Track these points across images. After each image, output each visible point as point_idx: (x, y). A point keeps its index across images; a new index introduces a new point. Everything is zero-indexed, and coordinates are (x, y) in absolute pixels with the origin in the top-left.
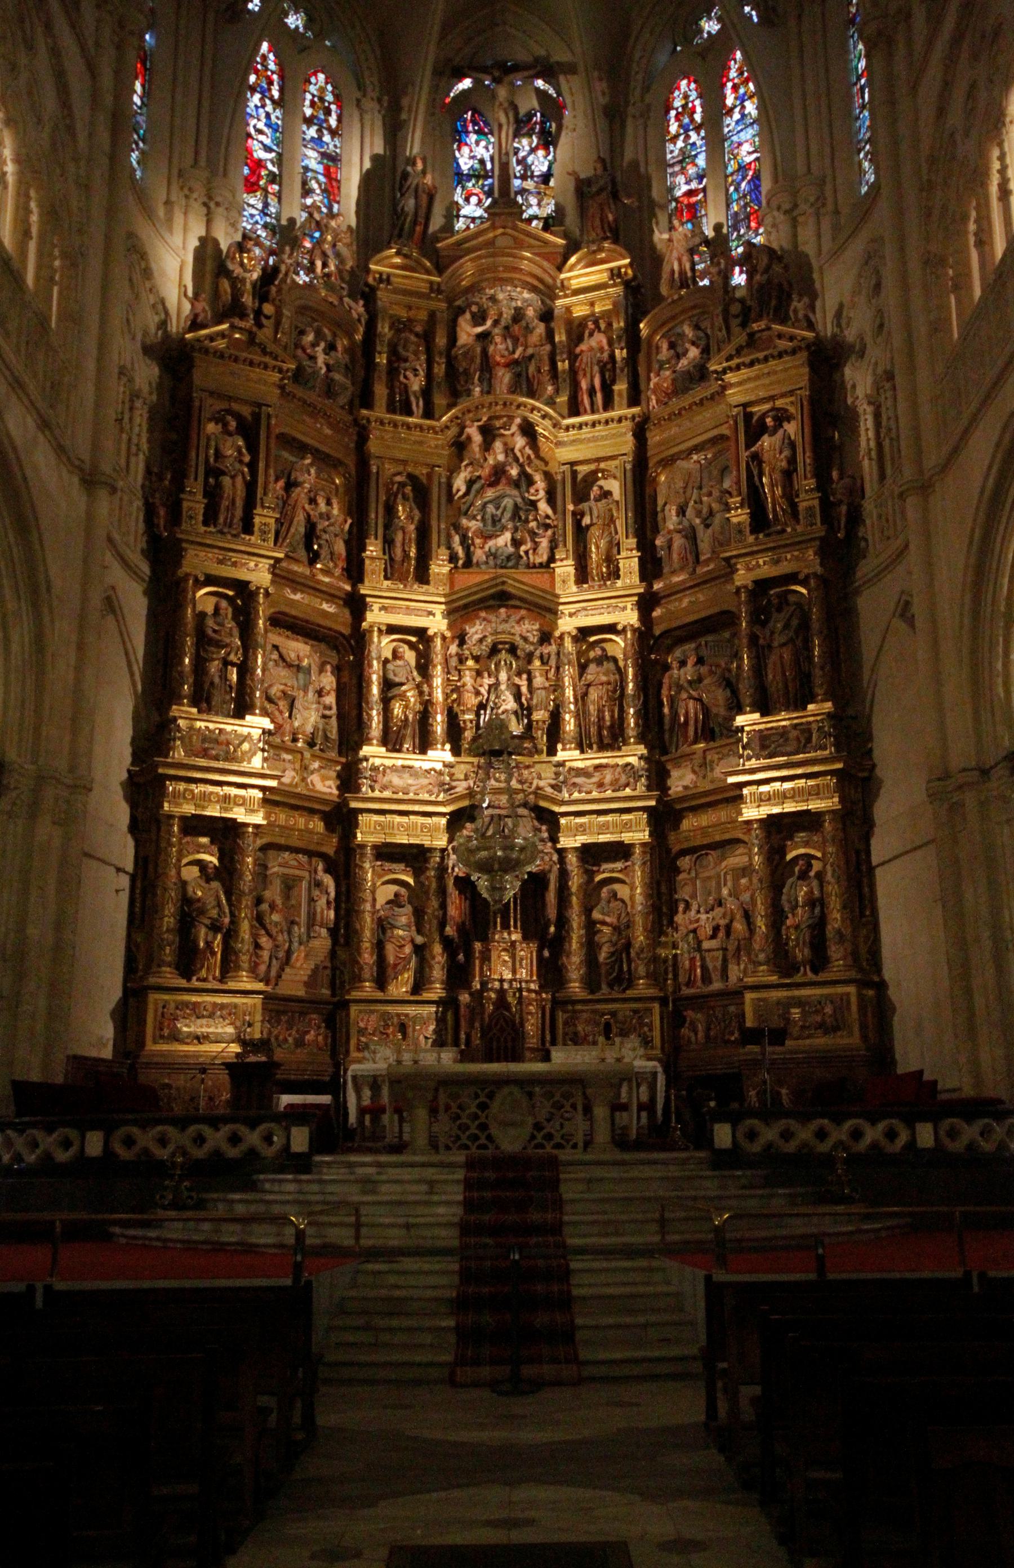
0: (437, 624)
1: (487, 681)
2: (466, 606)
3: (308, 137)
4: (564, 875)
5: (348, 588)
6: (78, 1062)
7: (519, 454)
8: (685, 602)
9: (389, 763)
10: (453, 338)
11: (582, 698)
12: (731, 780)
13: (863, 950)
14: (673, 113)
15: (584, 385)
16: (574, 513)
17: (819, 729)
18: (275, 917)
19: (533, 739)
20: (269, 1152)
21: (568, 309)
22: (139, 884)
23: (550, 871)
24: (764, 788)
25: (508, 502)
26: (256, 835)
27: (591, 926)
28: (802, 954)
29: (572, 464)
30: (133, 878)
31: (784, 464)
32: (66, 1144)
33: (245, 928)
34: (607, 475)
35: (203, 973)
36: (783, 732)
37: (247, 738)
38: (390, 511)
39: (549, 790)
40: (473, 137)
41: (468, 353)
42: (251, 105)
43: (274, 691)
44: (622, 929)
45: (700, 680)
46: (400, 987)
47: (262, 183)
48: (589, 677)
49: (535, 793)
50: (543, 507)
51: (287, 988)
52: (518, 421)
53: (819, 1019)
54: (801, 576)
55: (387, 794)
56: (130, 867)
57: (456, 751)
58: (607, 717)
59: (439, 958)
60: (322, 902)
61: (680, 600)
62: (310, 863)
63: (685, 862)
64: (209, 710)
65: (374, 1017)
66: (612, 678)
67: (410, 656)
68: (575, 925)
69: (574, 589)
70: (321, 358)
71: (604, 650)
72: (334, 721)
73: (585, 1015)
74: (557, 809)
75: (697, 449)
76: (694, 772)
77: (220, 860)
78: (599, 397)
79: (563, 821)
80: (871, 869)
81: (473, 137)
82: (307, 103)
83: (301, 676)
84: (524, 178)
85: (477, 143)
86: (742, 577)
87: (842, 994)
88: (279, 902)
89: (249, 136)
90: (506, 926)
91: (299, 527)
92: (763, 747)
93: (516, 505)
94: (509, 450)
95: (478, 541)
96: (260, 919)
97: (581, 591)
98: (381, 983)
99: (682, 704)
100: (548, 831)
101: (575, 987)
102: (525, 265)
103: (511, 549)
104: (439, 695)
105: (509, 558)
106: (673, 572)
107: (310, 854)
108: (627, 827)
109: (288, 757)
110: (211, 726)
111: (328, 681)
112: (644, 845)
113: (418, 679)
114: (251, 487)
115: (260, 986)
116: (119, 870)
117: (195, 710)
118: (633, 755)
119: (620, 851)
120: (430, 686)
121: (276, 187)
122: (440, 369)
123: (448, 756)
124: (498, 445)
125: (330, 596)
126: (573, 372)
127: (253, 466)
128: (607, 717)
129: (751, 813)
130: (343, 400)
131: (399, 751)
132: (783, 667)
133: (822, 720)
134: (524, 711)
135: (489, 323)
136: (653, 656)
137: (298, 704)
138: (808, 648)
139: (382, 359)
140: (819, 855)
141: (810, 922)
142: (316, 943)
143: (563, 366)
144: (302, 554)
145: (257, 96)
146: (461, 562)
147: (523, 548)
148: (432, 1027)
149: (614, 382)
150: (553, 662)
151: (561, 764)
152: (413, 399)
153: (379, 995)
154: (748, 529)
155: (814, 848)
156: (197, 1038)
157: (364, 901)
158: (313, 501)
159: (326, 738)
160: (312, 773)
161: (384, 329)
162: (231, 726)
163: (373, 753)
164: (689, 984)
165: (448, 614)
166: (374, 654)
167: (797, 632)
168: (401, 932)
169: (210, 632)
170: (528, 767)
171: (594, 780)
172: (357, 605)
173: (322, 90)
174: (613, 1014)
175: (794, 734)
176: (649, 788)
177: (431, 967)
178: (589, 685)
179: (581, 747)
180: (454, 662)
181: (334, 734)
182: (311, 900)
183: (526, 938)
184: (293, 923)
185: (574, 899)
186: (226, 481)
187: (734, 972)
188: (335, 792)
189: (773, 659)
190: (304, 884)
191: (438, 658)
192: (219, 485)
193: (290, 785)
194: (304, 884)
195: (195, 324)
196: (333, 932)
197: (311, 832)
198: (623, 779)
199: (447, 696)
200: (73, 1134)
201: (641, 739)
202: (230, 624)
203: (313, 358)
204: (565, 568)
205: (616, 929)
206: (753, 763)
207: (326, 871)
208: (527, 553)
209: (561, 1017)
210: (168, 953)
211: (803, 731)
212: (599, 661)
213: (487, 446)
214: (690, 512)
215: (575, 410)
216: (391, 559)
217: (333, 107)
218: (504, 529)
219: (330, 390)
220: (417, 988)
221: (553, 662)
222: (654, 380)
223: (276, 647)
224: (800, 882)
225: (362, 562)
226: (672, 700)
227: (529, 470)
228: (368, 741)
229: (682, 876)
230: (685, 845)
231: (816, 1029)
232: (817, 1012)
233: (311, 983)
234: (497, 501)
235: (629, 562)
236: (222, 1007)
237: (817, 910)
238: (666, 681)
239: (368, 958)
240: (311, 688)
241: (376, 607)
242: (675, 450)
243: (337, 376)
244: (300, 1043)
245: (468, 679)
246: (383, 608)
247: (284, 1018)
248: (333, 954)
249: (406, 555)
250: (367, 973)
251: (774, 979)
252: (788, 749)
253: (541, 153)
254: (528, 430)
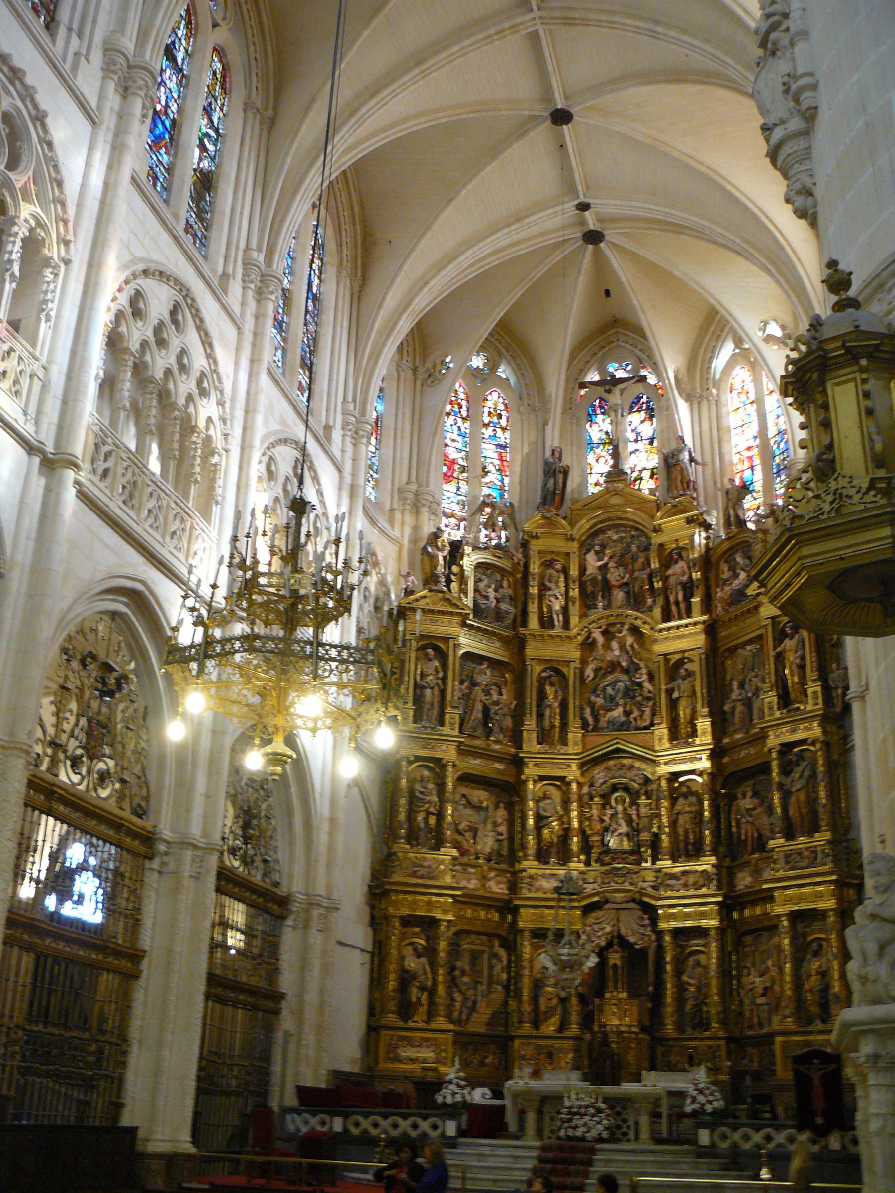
0: (573, 772)
1: (609, 812)
2: (593, 759)
3: (486, 437)
4: (660, 949)
5: (513, 750)
6: (336, 1074)
7: (629, 648)
8: (743, 754)
9: (540, 872)
10: (583, 569)
11: (673, 824)
12: (765, 886)
14: (735, 392)
15: (672, 598)
16: (667, 691)
18: (466, 979)
19: (638, 852)
20: (434, 1134)
21: (661, 545)
22: (376, 959)
23: (649, 948)
24: (788, 892)
25: (620, 685)
26: (448, 926)
27: (681, 987)
28: (814, 1009)
29: (665, 655)
30: (373, 954)
31: (798, 661)
32: (323, 1124)
33: (441, 990)
34: (691, 660)
35: (416, 1018)
36: (799, 853)
37: (442, 862)
38: (542, 696)
39: (650, 890)
40: (600, 417)
41: (594, 579)
42: (448, 424)
43: (462, 826)
44: (702, 988)
45: (754, 809)
46: (550, 1028)
47: (455, 475)
48: (678, 807)
49: (639, 892)
50: (647, 685)
51: (471, 1028)
52: (627, 627)
54: (809, 741)
55: (539, 895)
56: (370, 949)
57: (587, 863)
58: (691, 836)
59: (576, 1008)
60: (498, 969)
61: (739, 752)
62: (489, 941)
63: (749, 939)
64: (418, 845)
65: (531, 1048)
66: (693, 809)
67: (556, 795)
68: (669, 985)
69: (667, 745)
70: (492, 594)
71: (688, 788)
72: (505, 843)
73: (675, 1049)
74: (654, 902)
75: (750, 642)
76: (751, 876)
77: (427, 941)
78: (682, 606)
79: (660, 911)
81: (600, 417)
82: (486, 414)
83: (482, 813)
84: (636, 441)
85: (603, 420)
86: (773, 741)
88: (467, 968)
89: (446, 445)
90: (616, 988)
91: (478, 713)
92: (787, 863)
93: (626, 687)
94: (622, 647)
95: (602, 712)
96: (453, 983)
97: (674, 747)
98: (536, 1025)
99: (743, 826)
100: (650, 918)
101: (669, 1029)
102: (629, 516)
103: (623, 719)
104: (576, 824)
105: (622, 724)
106: (735, 732)
107: (490, 935)
108: (703, 915)
109: (472, 870)
110: (418, 856)
111: (501, 814)
112: (716, 928)
113: (561, 813)
114: (443, 692)
115: (451, 1027)
116: (363, 951)
117: (408, 846)
118: (707, 863)
119: (700, 932)
120: (569, 817)
121: (465, 475)
122: (575, 592)
123: (581, 866)
124: (614, 645)
125: (500, 759)
126: (665, 589)
127: (444, 679)
128: (691, 836)
129: (779, 910)
130: (509, 621)
131: (547, 863)
134: (633, 832)
135: (606, 559)
136: (723, 791)
137: (479, 834)
138: (815, 790)
139: (534, 591)
142: (494, 996)
143: (658, 585)
144: (479, 732)
145: (452, 418)
146: (590, 727)
147: (632, 716)
148: (571, 1056)
149: (692, 596)
150: (654, 797)
151: (659, 871)
152: (555, 616)
153: (535, 1033)
154: (776, 707)
156: (411, 1060)
157: (524, 968)
158: (487, 693)
159: (500, 855)
160: (490, 880)
161: (535, 568)
162: (431, 856)
163: (530, 865)
164: (751, 1027)
165: (581, 766)
166: (530, 797)
167: (808, 783)
168: (550, 989)
169: (418, 794)
170: (637, 873)
171: (682, 882)
172: (518, 763)
173: (496, 403)
174: (695, 1048)
175: (807, 853)
176: (719, 888)
177: (570, 1013)
178: (678, 814)
179: (674, 859)
180: (585, 799)
181: (505, 852)
182: (491, 967)
183: (631, 995)
184: (477, 982)
185: (669, 968)
186: (428, 692)
187: (776, 1019)
188: (506, 892)
189: (793, 799)
190: (486, 956)
191: (574, 797)
192: (422, 696)
193: (474, 890)
194: (486, 956)
195: (408, 592)
196: (506, 987)
197: (489, 920)
198: (701, 882)
199: (581, 823)
200: (327, 1118)
201: (715, 852)
202: (431, 786)
203: (486, 597)
204: (662, 731)
205: (699, 988)
206: (781, 874)
207: (502, 946)
208: (635, 719)
209: (660, 1050)
210: (392, 1005)
212: (685, 796)
213: (607, 647)
214: (747, 687)
215: (667, 617)
216: (543, 729)
217: (504, 413)
218: (617, 705)
219: (499, 616)
220: (562, 1028)
221: (654, 797)
222: (719, 594)
223: (464, 796)
225: (521, 732)
226: (738, 823)
227: (635, 660)
228: (525, 857)
229: (747, 949)
230: (747, 928)
233: (490, 1024)
234: (613, 684)
235: (704, 724)
236: (427, 1040)
238: (734, 808)
239: (527, 1007)
240: (489, 821)
241: (531, 765)
242: (736, 642)
243: (504, 606)
244: (482, 1064)
245: (595, 812)
246: (536, 765)
247: (471, 1047)
248: (505, 1003)
249: (553, 726)
250: (526, 1018)
251: (793, 1027)
252: (803, 864)
253: (648, 423)
254: (635, 631)
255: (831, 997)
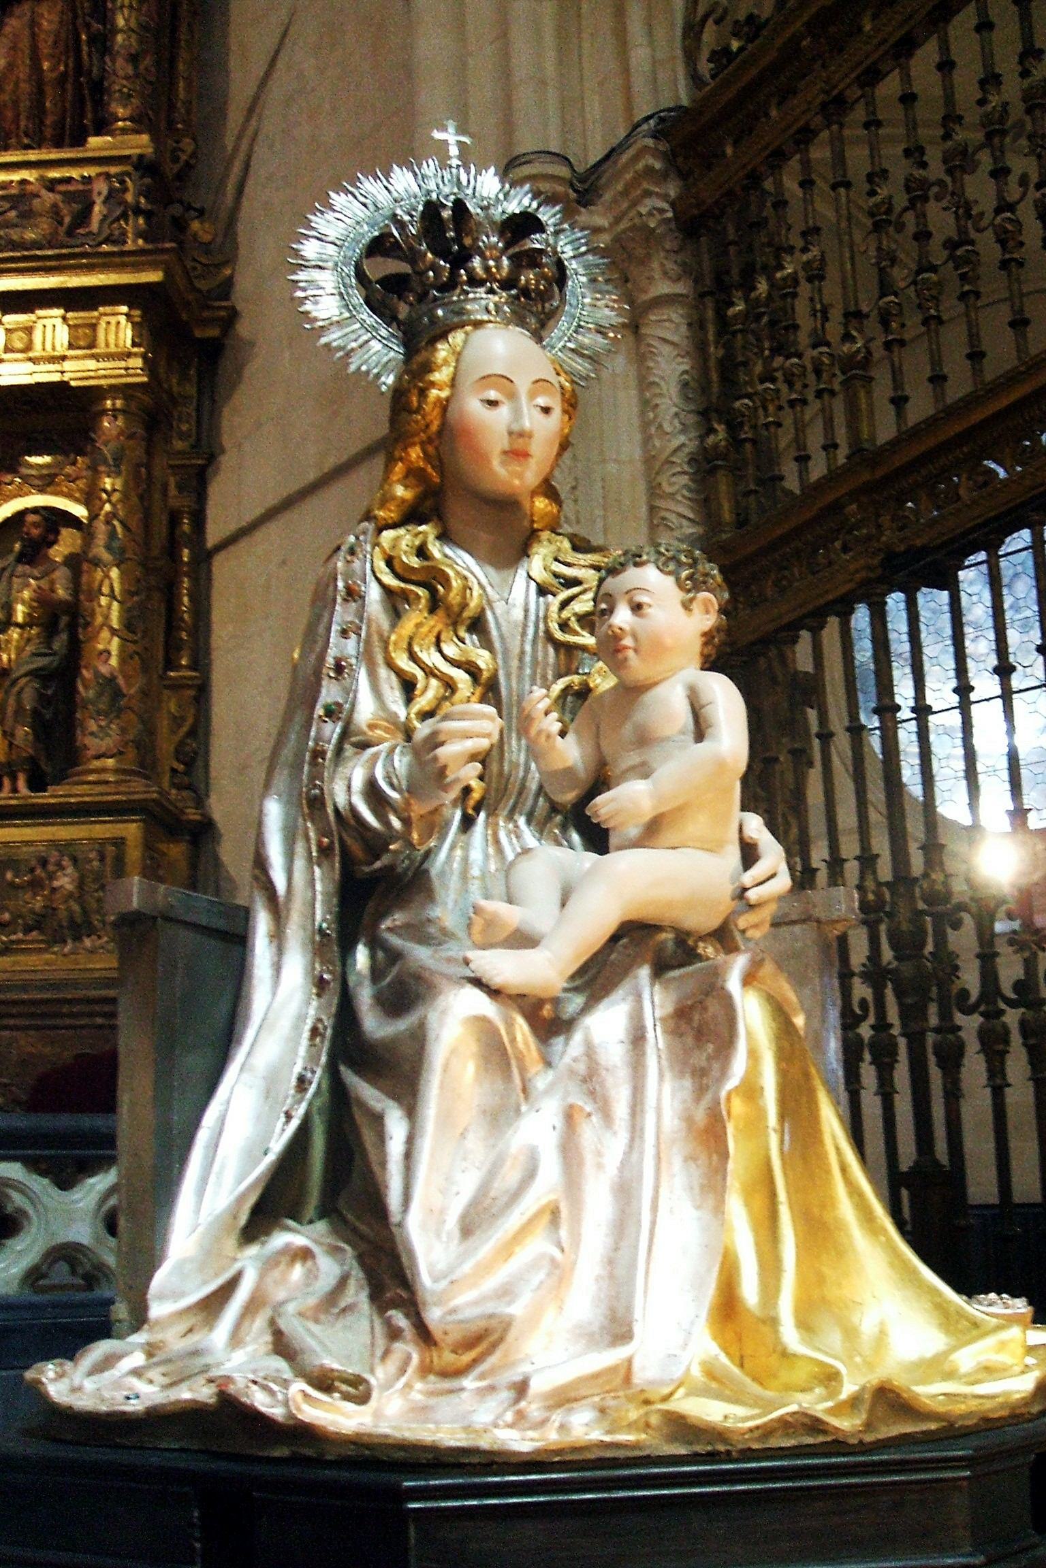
13: (166, 744)
17: (111, 194)
53: (38, 903)
80: (204, 558)
87: (104, 842)
132: (34, 49)
133: (121, 178)
140: (80, 511)
141: (41, 662)
155: (69, 496)
211: (69, 197)
224: (20, 569)
231: (28, 930)
232: (35, 885)
237: (60, 642)
252: (30, 235)
255: (86, 692)
